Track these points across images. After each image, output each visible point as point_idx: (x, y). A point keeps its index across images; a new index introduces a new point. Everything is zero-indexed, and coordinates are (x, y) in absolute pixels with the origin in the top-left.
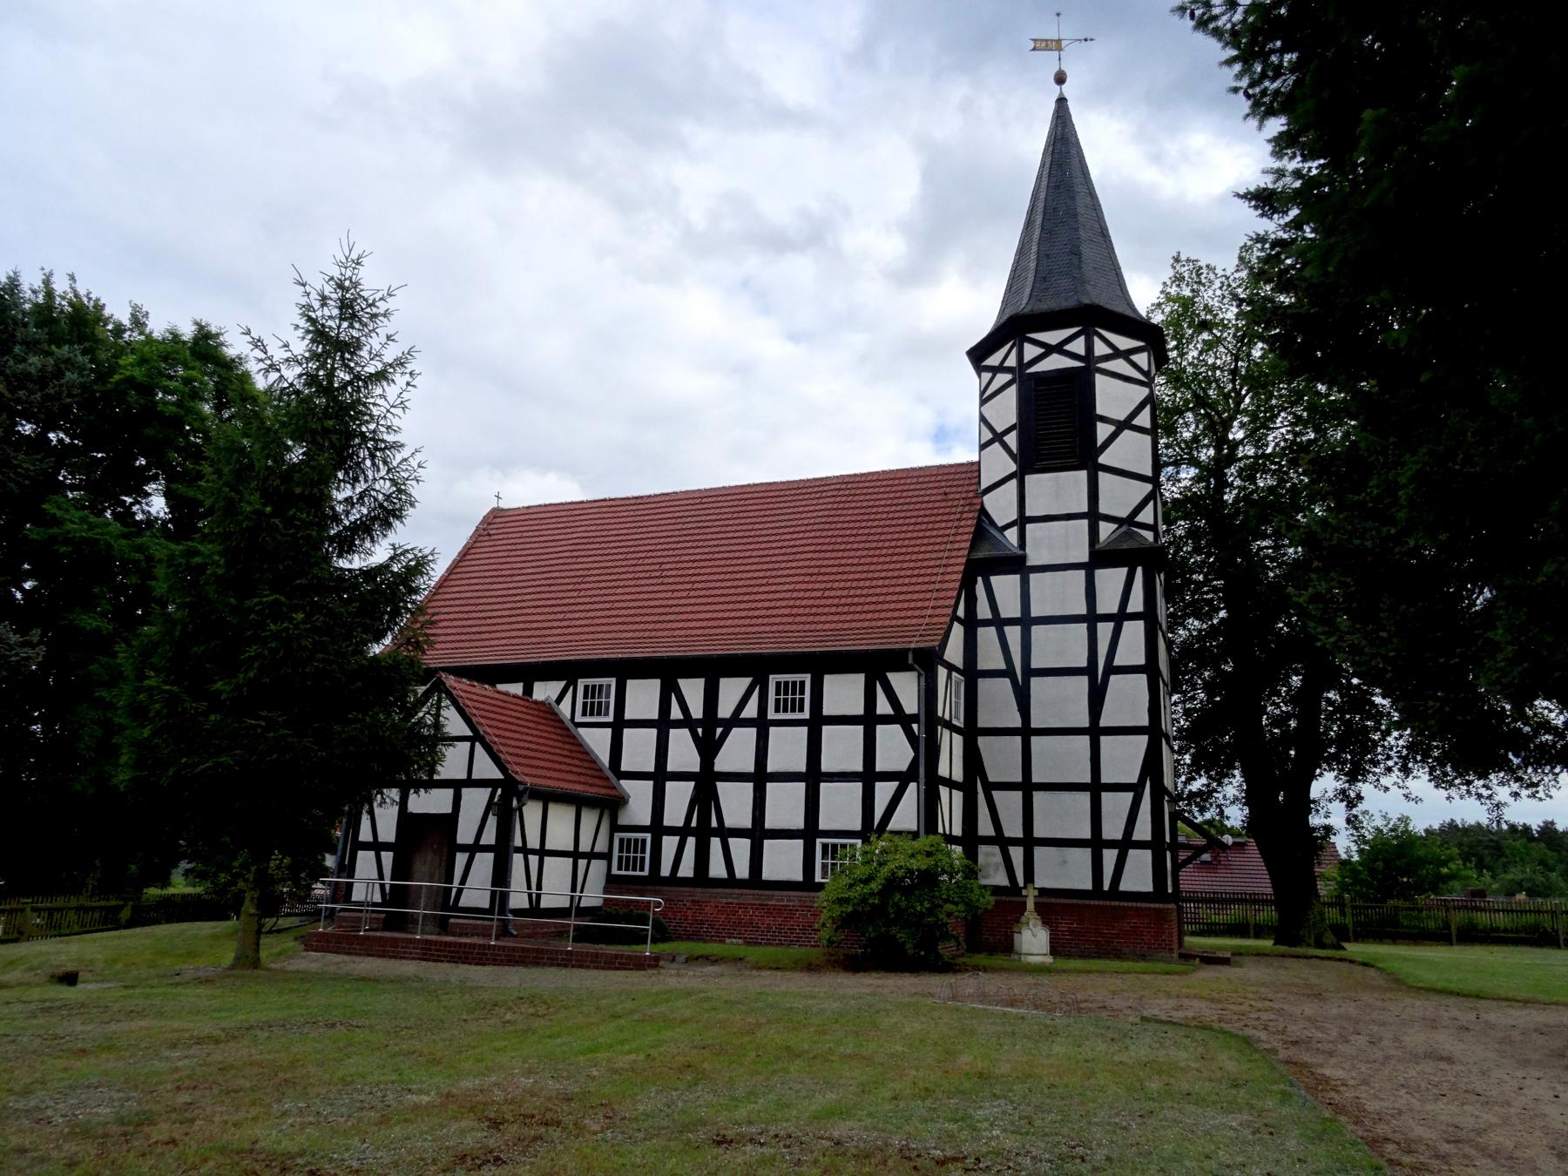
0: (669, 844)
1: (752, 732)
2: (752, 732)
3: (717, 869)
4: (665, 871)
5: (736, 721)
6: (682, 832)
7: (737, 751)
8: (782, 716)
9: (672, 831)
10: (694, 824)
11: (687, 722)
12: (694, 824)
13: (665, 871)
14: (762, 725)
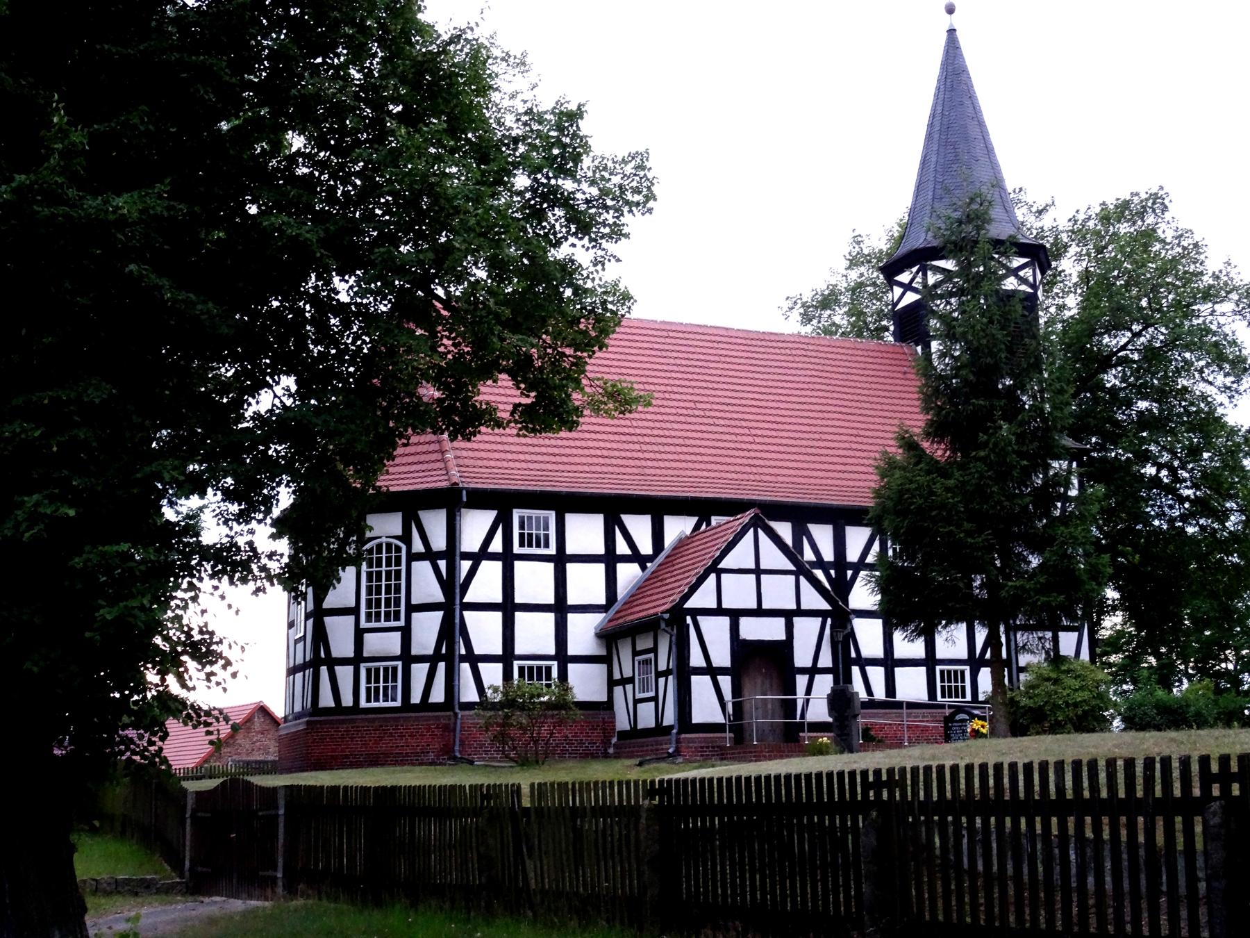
0: (419, 672)
1: (497, 566)
2: (497, 566)
3: (469, 694)
4: (416, 698)
5: (483, 554)
6: (432, 660)
7: (486, 583)
8: (526, 550)
9: (421, 659)
10: (444, 651)
11: (430, 555)
12: (444, 651)
13: (416, 698)
14: (508, 559)
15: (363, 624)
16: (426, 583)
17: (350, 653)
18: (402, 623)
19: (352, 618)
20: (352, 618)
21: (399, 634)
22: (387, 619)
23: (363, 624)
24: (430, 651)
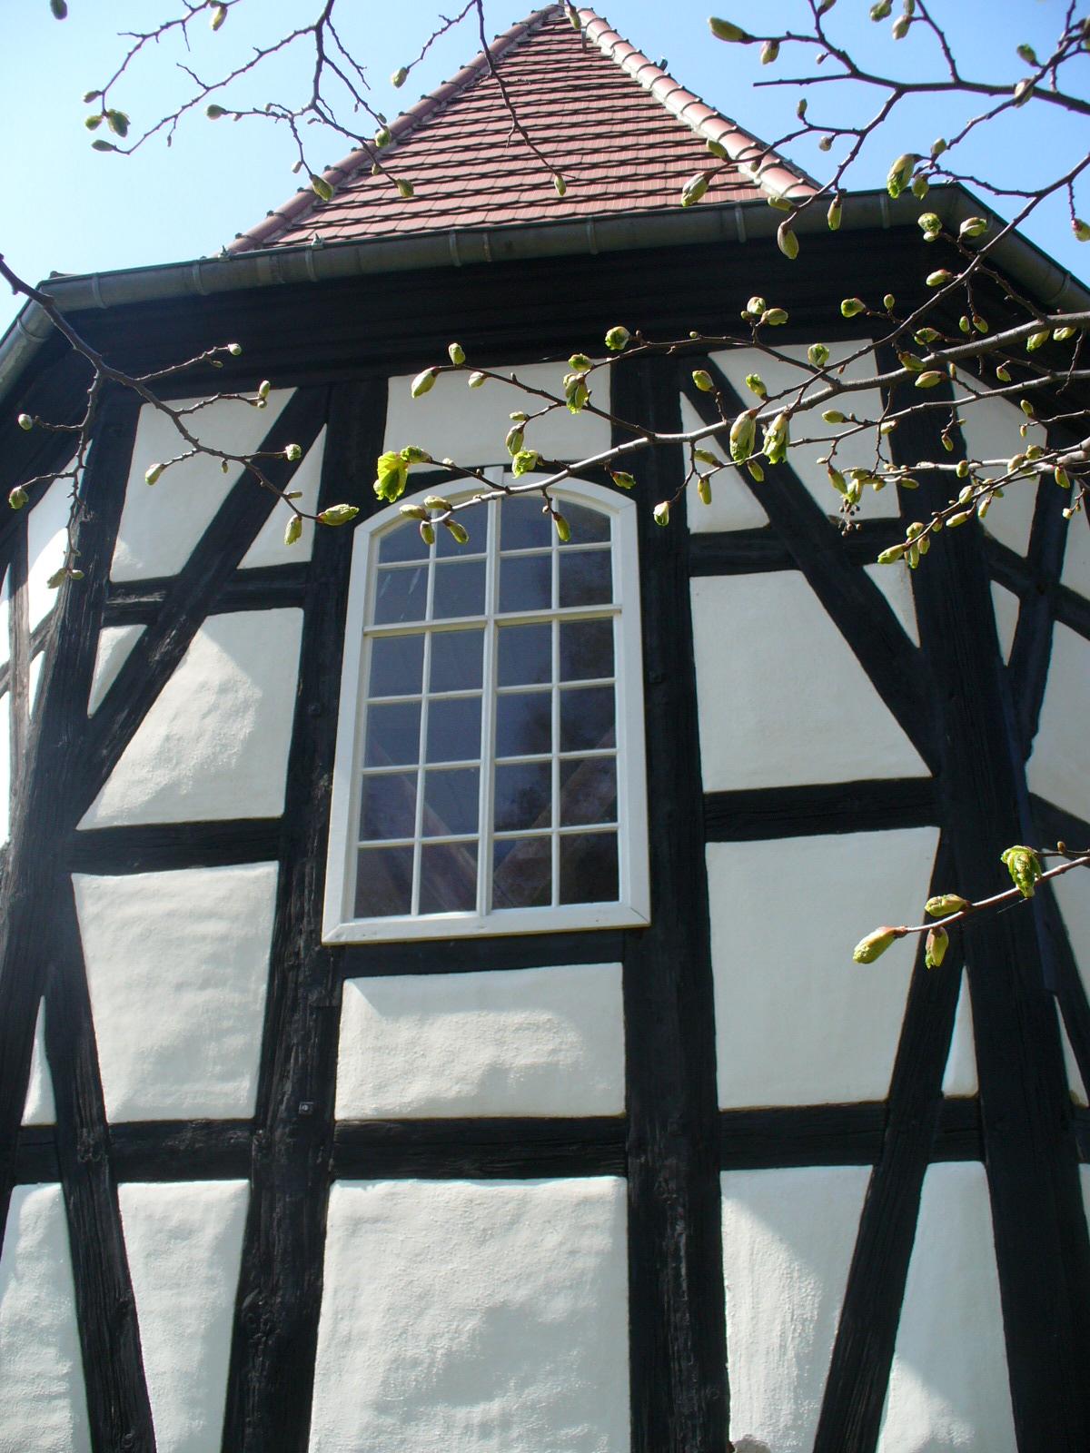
6: (887, 1139)
15: (338, 923)
16: (784, 686)
17: (230, 1092)
18: (631, 904)
19: (257, 881)
20: (257, 881)
21: (606, 979)
22: (520, 882)
23: (338, 923)
24: (866, 1075)
